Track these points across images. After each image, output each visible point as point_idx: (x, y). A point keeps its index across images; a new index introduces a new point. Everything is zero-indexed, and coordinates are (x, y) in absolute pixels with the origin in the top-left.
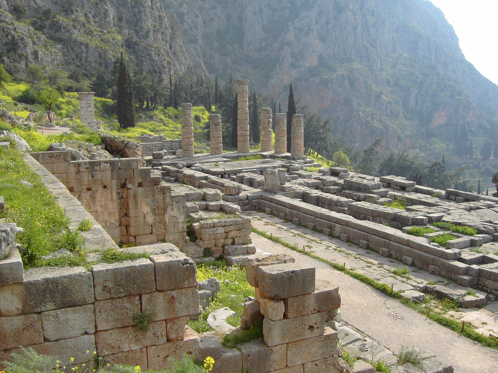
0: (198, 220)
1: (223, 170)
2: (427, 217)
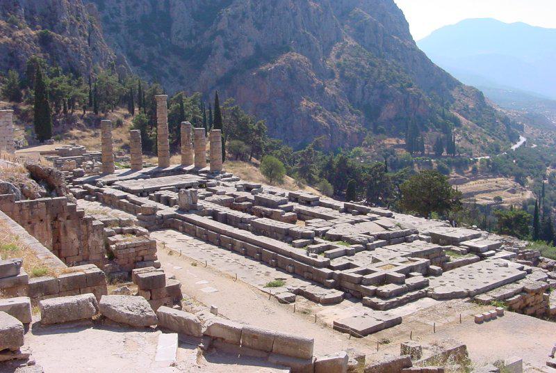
0: (114, 243)
1: (142, 188)
2: (315, 231)
